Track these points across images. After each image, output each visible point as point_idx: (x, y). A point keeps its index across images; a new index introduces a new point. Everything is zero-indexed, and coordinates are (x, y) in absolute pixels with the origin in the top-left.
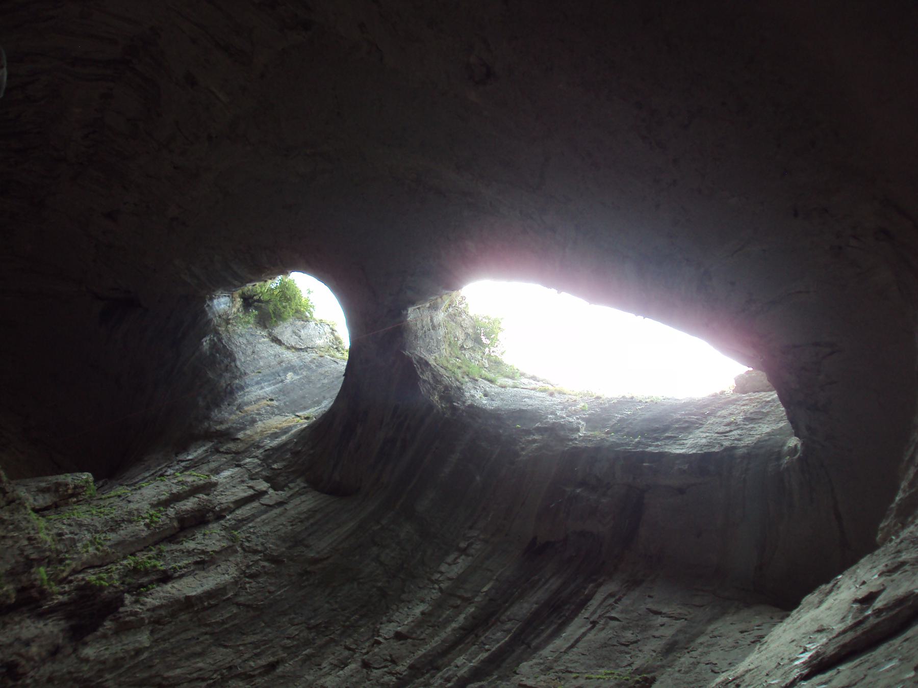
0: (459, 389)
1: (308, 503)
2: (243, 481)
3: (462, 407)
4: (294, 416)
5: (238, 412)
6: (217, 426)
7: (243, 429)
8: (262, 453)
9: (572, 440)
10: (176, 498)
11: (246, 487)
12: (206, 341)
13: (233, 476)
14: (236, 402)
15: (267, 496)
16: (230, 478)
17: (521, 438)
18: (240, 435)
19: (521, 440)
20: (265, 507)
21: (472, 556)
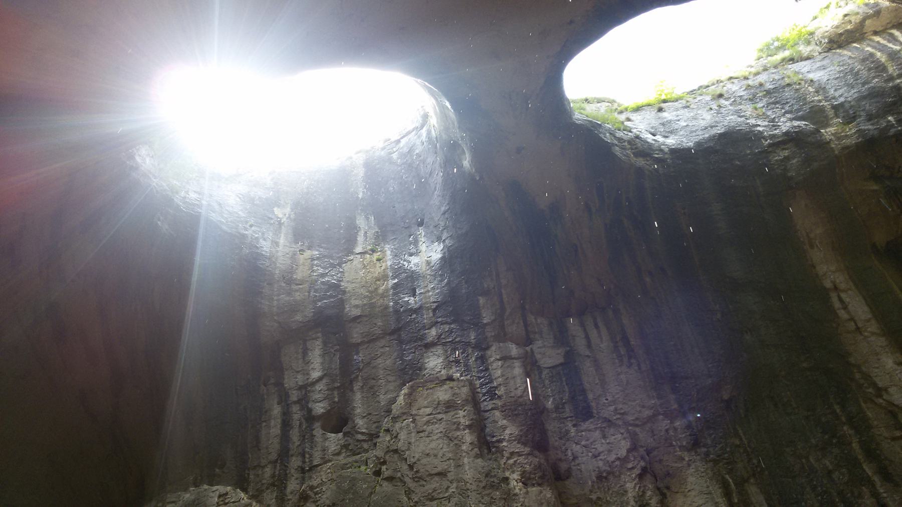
0: (637, 137)
1: (593, 334)
2: (482, 359)
3: (667, 156)
4: (359, 256)
5: (295, 287)
6: (294, 317)
7: (342, 303)
8: (434, 315)
9: (828, 143)
10: (479, 426)
11: (500, 363)
12: (159, 220)
13: (451, 360)
14: (276, 276)
15: (538, 356)
16: (453, 364)
17: (771, 161)
18: (356, 312)
19: (772, 163)
20: (560, 368)
21: (849, 289)
